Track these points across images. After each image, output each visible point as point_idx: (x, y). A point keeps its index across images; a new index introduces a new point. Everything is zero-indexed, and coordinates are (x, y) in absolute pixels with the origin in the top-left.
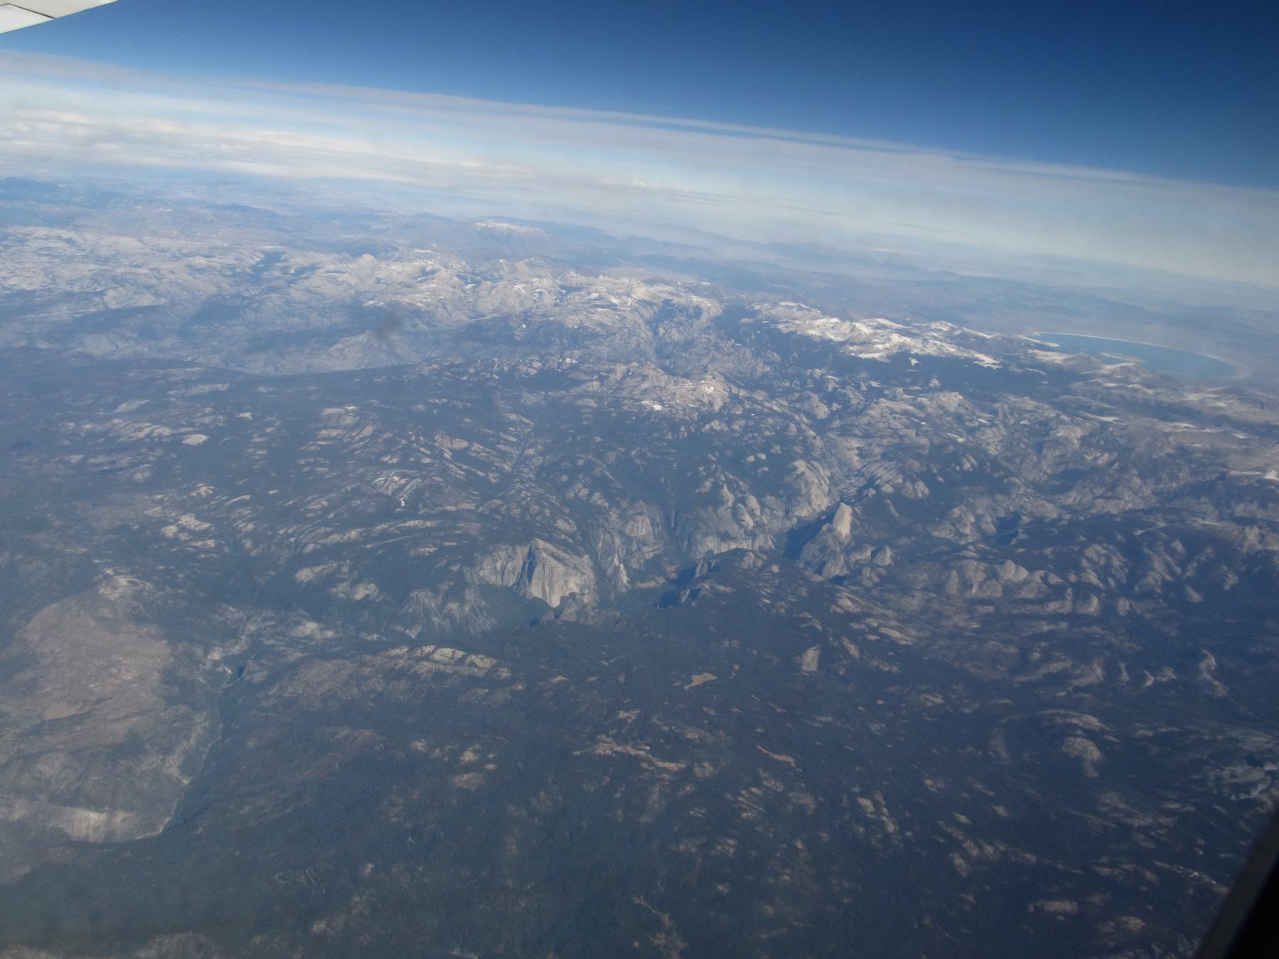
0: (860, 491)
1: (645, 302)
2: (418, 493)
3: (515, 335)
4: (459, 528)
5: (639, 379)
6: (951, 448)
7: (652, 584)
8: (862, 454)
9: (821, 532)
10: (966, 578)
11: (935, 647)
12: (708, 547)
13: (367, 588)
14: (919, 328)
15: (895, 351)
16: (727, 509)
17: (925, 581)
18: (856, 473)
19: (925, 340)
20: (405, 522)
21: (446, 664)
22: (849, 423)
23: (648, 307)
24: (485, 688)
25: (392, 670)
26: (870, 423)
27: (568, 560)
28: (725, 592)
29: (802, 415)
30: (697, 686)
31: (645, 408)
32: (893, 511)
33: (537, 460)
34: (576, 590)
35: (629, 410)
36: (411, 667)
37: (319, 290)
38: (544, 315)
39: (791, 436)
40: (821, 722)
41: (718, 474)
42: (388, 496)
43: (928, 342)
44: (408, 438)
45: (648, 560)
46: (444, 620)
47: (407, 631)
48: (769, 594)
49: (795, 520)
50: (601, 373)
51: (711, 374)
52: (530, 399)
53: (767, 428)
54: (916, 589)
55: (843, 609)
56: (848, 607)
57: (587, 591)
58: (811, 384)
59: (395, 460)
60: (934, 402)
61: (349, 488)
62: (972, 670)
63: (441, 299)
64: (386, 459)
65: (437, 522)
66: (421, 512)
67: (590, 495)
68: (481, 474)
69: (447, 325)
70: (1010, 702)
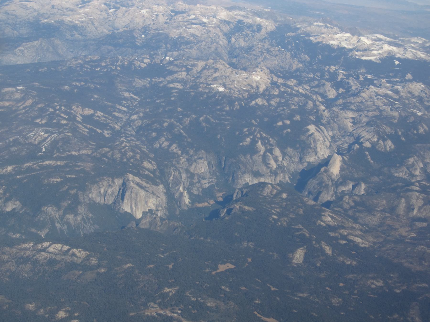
0: (350, 146)
1: (225, 21)
2: (55, 143)
3: (137, 42)
4: (79, 166)
5: (212, 71)
6: (412, 119)
7: (206, 204)
8: (355, 122)
9: (320, 172)
10: (411, 204)
11: (384, 249)
12: (245, 181)
13: (15, 204)
14: (403, 41)
15: (385, 55)
16: (259, 156)
17: (384, 205)
18: (349, 134)
19: (405, 49)
20: (43, 162)
21: (56, 254)
22: (348, 101)
23: (227, 25)
24: (80, 270)
25: (22, 257)
26: (362, 102)
27: (148, 188)
28: (248, 210)
29: (318, 96)
30: (220, 272)
31: (213, 90)
32: (370, 159)
33: (138, 122)
34: (153, 207)
35: (203, 90)
36: (34, 255)
37: (14, 13)
38: (157, 29)
39: (308, 109)
40: (300, 297)
41: (256, 133)
42: (35, 145)
43: (407, 50)
44: (54, 108)
45: (205, 189)
46: (64, 226)
47: (39, 232)
48: (278, 212)
49: (306, 164)
50: (188, 67)
51: (261, 68)
52: (139, 83)
53: (293, 104)
54: (377, 211)
55: (325, 223)
56: (329, 222)
57: (160, 208)
58: (328, 75)
59: (44, 122)
60: (406, 89)
61: (11, 139)
62: (406, 265)
63: (91, 18)
64: (38, 121)
65: (65, 162)
66: (55, 155)
67: (169, 146)
68: (99, 131)
69: (94, 36)
70: (427, 285)
